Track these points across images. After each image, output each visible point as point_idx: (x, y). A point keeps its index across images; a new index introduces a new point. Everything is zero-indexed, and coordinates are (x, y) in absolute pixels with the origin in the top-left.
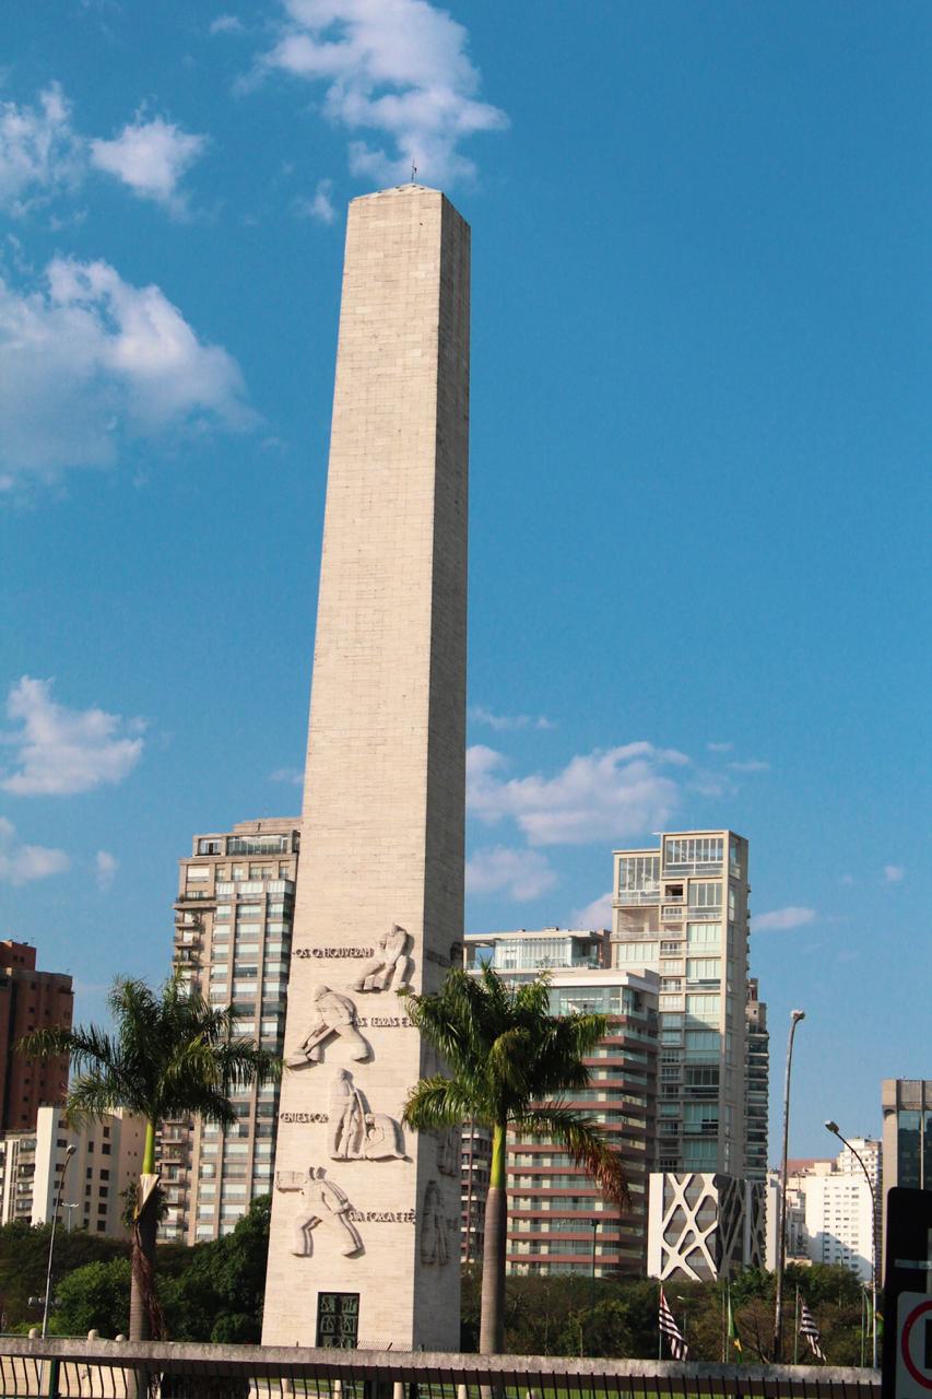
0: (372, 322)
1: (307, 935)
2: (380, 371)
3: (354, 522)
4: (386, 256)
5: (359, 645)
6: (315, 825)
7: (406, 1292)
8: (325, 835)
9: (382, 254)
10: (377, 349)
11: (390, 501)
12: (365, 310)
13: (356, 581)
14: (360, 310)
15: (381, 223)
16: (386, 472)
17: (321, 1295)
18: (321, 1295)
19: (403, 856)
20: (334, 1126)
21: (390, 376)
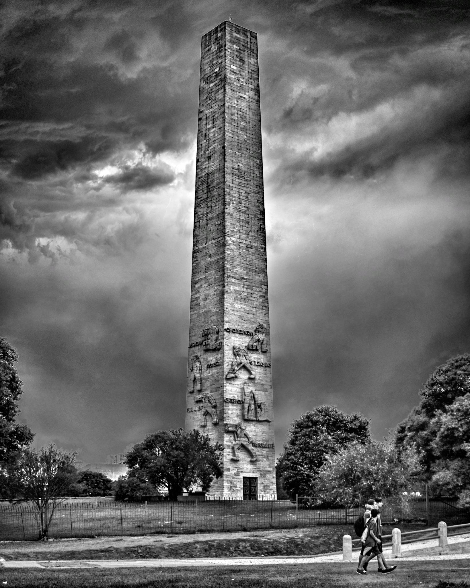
0: (237, 74)
1: (229, 322)
2: (241, 94)
3: (235, 153)
4: (240, 49)
5: (240, 204)
6: (230, 276)
7: (273, 477)
8: (233, 281)
9: (238, 48)
10: (239, 85)
11: (247, 149)
12: (235, 68)
13: (238, 177)
14: (232, 66)
15: (238, 36)
16: (246, 137)
17: (244, 478)
18: (244, 478)
19: (261, 296)
20: (246, 406)
21: (244, 98)
